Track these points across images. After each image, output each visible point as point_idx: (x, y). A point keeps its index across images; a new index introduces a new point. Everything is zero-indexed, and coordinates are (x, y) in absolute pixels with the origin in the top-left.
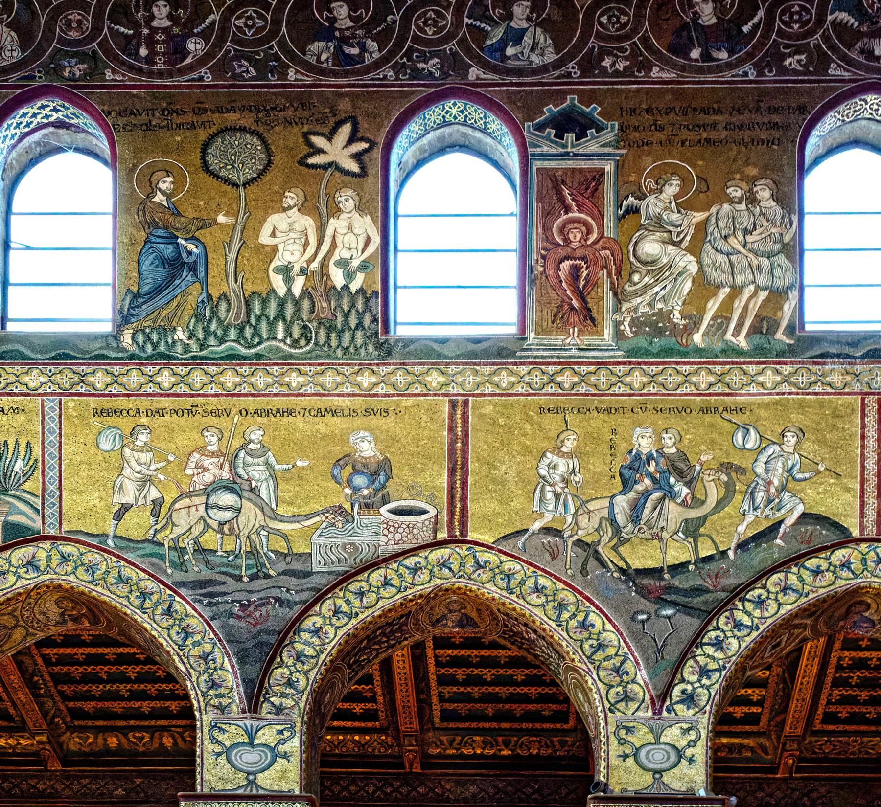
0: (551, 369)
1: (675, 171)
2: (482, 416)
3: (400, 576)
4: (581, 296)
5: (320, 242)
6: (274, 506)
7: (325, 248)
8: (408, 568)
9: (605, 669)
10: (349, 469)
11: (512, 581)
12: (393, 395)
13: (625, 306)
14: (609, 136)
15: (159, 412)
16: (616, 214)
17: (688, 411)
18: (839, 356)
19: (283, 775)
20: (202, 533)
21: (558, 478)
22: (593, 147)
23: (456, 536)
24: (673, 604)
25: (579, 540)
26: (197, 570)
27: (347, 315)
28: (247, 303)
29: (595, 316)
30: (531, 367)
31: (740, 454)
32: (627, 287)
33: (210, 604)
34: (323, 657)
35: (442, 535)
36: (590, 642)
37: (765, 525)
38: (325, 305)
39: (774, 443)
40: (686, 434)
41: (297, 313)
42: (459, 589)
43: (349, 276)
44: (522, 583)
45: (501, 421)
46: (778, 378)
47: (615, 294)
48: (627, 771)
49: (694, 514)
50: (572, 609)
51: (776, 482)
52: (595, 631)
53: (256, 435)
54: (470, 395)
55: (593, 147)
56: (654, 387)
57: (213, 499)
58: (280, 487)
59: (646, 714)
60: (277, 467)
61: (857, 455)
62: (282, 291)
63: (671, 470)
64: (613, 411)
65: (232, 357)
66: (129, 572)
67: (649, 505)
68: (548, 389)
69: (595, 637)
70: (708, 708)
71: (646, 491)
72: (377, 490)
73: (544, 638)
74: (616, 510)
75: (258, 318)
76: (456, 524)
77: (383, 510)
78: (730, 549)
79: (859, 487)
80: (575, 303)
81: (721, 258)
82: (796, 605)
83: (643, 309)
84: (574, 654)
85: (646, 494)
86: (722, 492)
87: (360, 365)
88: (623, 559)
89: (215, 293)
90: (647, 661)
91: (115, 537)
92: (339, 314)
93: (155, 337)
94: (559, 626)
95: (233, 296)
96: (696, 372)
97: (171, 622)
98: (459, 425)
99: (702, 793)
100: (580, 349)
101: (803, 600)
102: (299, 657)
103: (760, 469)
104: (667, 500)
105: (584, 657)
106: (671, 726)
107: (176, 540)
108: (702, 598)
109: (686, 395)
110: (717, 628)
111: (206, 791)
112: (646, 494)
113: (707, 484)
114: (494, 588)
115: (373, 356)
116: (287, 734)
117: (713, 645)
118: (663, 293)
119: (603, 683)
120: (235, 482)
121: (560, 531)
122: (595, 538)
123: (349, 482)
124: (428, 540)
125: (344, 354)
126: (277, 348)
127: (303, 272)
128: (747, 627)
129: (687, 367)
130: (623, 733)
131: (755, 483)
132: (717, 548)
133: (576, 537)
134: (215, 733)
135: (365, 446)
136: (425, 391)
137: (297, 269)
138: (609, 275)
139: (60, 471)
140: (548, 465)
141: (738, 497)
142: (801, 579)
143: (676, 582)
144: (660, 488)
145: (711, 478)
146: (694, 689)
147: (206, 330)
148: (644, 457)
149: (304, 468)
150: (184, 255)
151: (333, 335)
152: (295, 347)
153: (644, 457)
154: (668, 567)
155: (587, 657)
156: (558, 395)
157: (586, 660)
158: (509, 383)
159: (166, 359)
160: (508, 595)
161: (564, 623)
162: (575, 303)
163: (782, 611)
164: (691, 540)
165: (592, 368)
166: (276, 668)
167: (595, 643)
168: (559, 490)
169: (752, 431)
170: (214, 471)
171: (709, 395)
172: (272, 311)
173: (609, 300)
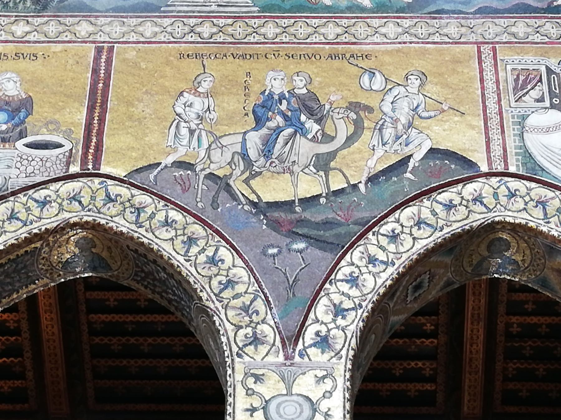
0: (192, 21)
2: (124, 60)
8: (36, 201)
9: (234, 308)
11: (142, 215)
12: (43, 42)
17: (318, 57)
18: (454, 12)
21: (193, 116)
23: (89, 169)
25: (210, 173)
30: (174, 19)
31: (367, 94)
36: (219, 278)
37: (394, 159)
39: (399, 85)
40: (316, 77)
42: (87, 222)
44: (152, 216)
45: (143, 65)
46: (400, 30)
50: (202, 243)
51: (403, 120)
52: (225, 266)
54: (116, 43)
56: (286, 37)
59: (277, 360)
61: (478, 96)
63: (303, 109)
64: (248, 57)
67: (281, 140)
68: (188, 38)
69: (225, 273)
70: (344, 352)
71: (278, 127)
72: (17, 125)
73: (172, 276)
76: (90, 157)
78: (360, 182)
79: (483, 125)
82: (431, 239)
84: (201, 291)
85: (278, 130)
86: (351, 129)
87: (16, 16)
88: (254, 192)
90: (278, 298)
94: (187, 261)
96: (324, 25)
98: (103, 68)
100: (219, 6)
101: (438, 234)
103: (387, 108)
104: (298, 135)
105: (212, 295)
106: (304, 374)
108: (334, 232)
109: (315, 43)
112: (278, 130)
113: (335, 120)
114: (123, 222)
115: (30, 10)
117: (347, 281)
119: (232, 324)
121: (193, 165)
122: (227, 171)
125: (4, 7)
128: (382, 262)
129: (317, 21)
130: (251, 380)
131: (383, 120)
132: (348, 182)
133: (208, 171)
135: (10, 85)
136: (74, 39)
140: (185, 104)
142: (434, 213)
143: (307, 215)
144: (292, 125)
145: (341, 116)
146: (329, 331)
148: (276, 97)
153: (276, 97)
154: (300, 200)
155: (215, 294)
156: (198, 43)
157: (214, 298)
158: (152, 32)
160: (136, 229)
161: (193, 258)
164: (322, 173)
165: (230, 21)
167: (224, 280)
168: (193, 126)
169: (377, 74)
171: (338, 43)
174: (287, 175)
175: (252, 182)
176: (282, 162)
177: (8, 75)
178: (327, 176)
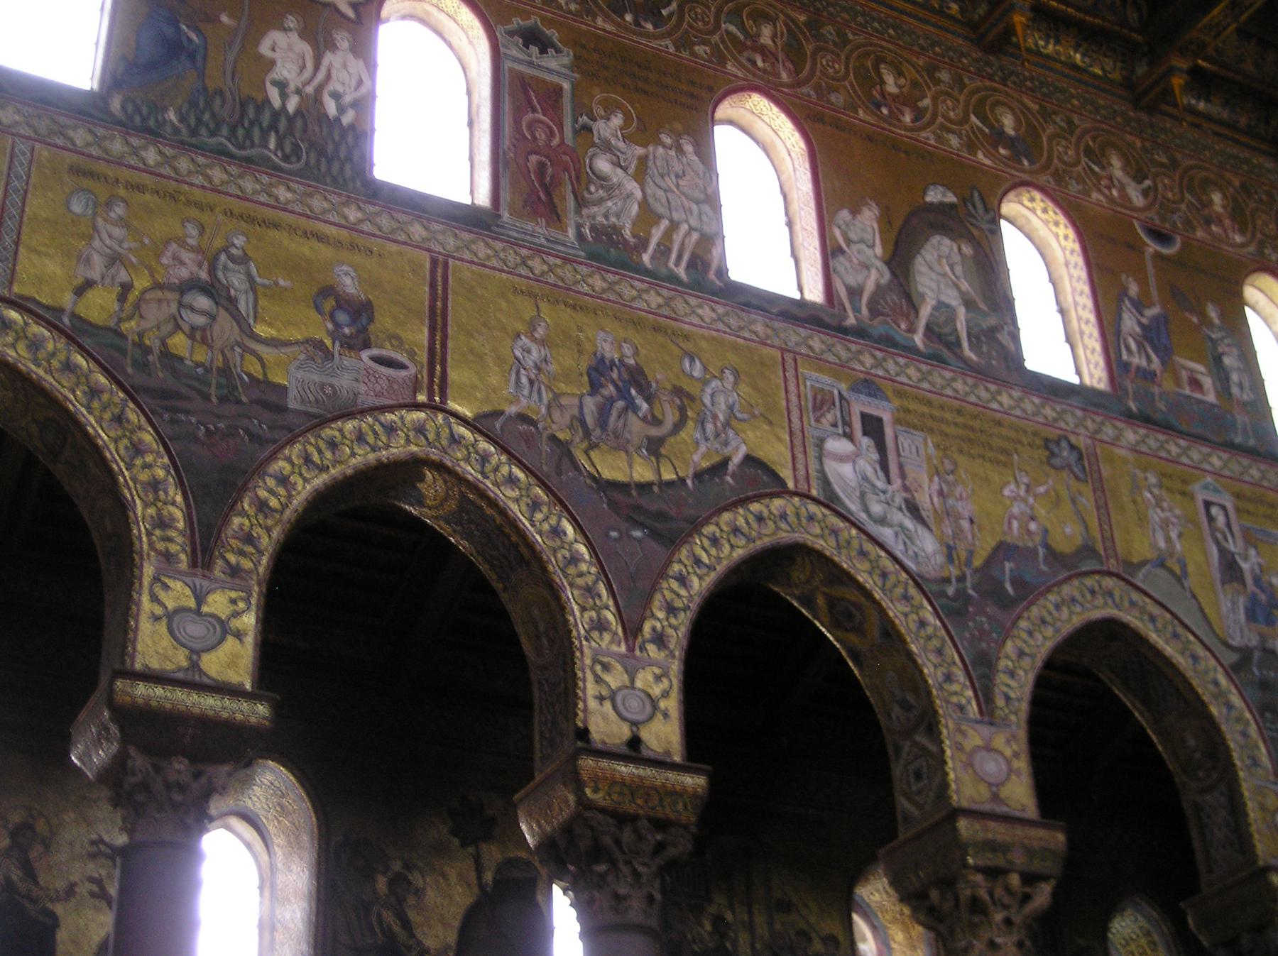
0: (524, 252)
1: (619, 106)
3: (375, 433)
4: (548, 194)
5: (317, 68)
6: (251, 321)
7: (321, 75)
10: (329, 304)
13: (585, 211)
14: (566, 61)
15: (140, 188)
16: (573, 128)
19: (232, 663)
20: (172, 334)
21: (531, 363)
22: (553, 64)
24: (642, 526)
26: (161, 376)
27: (337, 147)
28: (243, 105)
29: (560, 212)
32: (587, 196)
33: (173, 422)
34: (288, 513)
35: (422, 398)
36: (563, 551)
38: (317, 129)
39: (716, 377)
41: (290, 130)
43: (341, 109)
44: (496, 470)
47: (576, 198)
48: (605, 718)
49: (654, 432)
51: (721, 418)
53: (239, 241)
55: (553, 64)
57: (188, 298)
58: (260, 302)
60: (258, 280)
62: (276, 101)
65: (220, 153)
66: (80, 360)
67: (614, 413)
72: (359, 332)
74: (586, 411)
75: (252, 123)
76: (436, 387)
77: (365, 355)
80: (542, 196)
81: (660, 193)
83: (600, 219)
85: (611, 401)
89: (211, 87)
91: (74, 316)
92: (330, 142)
93: (145, 110)
95: (228, 94)
97: (120, 433)
99: (677, 758)
102: (262, 506)
107: (141, 335)
110: (680, 561)
111: (138, 666)
112: (611, 401)
116: (241, 605)
118: (614, 208)
120: (213, 286)
123: (332, 317)
124: (408, 401)
126: (269, 159)
127: (298, 92)
130: (598, 668)
133: (549, 431)
134: (158, 589)
137: (292, 87)
138: (570, 178)
139: (21, 223)
141: (690, 424)
143: (643, 501)
147: (199, 121)
148: (607, 362)
149: (285, 289)
150: (184, 40)
151: (323, 161)
152: (285, 162)
159: (153, 134)
162: (542, 196)
163: (735, 555)
165: (559, 262)
166: (235, 515)
168: (533, 376)
170: (189, 267)
171: (659, 315)
172: (266, 119)
173: (571, 203)
174: (622, 454)
175: (592, 454)
176: (617, 437)
177: (345, 268)
178: (658, 462)
